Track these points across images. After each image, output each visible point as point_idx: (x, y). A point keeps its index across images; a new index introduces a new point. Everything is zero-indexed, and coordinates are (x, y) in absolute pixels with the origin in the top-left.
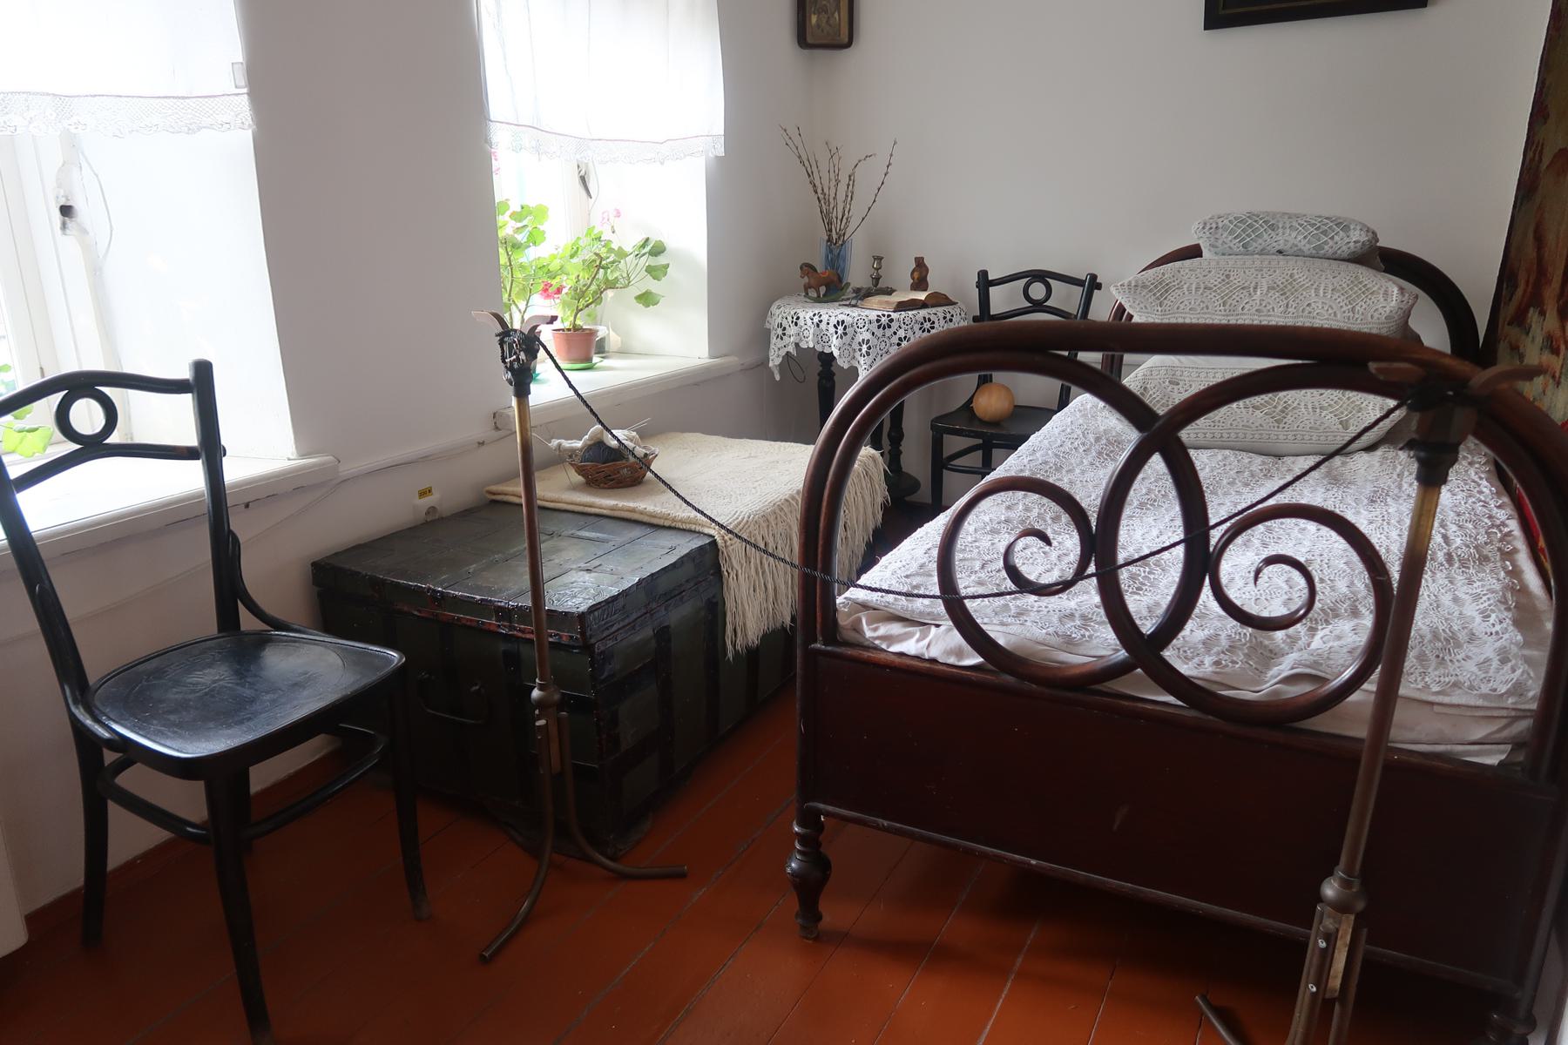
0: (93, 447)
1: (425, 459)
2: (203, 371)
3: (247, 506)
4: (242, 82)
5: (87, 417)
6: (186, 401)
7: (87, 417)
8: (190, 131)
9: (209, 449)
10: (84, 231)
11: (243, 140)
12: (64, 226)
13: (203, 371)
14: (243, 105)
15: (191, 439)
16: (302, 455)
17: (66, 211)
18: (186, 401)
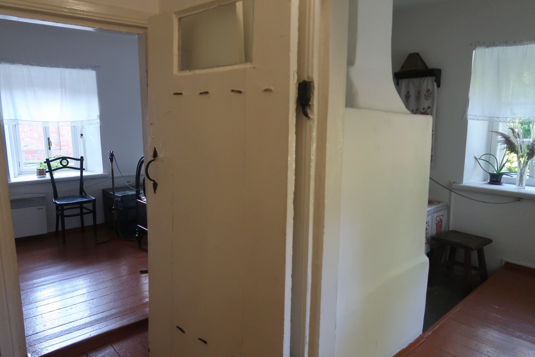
0: (65, 167)
1: (129, 176)
2: (82, 158)
3: (92, 179)
4: (99, 117)
5: (64, 163)
6: (79, 162)
7: (64, 163)
8: (90, 125)
9: (82, 169)
10: (84, 138)
11: (98, 126)
12: (81, 137)
13: (82, 158)
14: (98, 121)
15: (79, 167)
16: (104, 172)
17: (82, 135)
18: (79, 162)
